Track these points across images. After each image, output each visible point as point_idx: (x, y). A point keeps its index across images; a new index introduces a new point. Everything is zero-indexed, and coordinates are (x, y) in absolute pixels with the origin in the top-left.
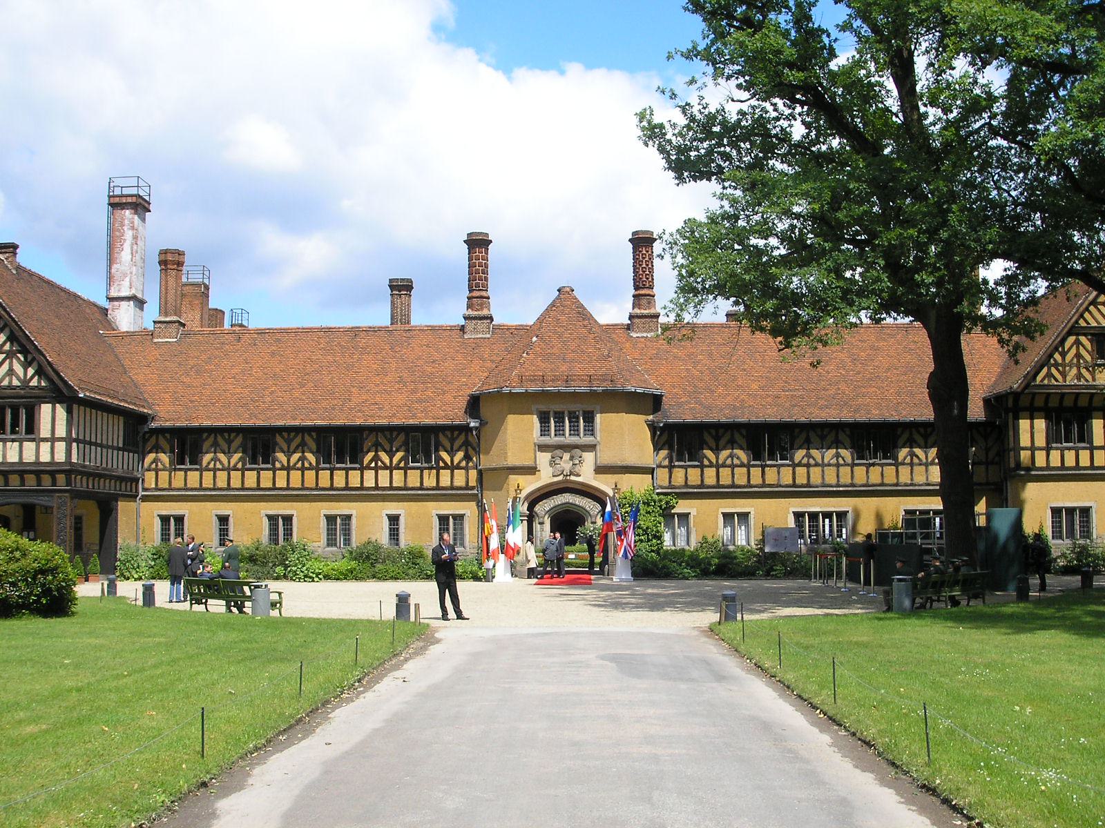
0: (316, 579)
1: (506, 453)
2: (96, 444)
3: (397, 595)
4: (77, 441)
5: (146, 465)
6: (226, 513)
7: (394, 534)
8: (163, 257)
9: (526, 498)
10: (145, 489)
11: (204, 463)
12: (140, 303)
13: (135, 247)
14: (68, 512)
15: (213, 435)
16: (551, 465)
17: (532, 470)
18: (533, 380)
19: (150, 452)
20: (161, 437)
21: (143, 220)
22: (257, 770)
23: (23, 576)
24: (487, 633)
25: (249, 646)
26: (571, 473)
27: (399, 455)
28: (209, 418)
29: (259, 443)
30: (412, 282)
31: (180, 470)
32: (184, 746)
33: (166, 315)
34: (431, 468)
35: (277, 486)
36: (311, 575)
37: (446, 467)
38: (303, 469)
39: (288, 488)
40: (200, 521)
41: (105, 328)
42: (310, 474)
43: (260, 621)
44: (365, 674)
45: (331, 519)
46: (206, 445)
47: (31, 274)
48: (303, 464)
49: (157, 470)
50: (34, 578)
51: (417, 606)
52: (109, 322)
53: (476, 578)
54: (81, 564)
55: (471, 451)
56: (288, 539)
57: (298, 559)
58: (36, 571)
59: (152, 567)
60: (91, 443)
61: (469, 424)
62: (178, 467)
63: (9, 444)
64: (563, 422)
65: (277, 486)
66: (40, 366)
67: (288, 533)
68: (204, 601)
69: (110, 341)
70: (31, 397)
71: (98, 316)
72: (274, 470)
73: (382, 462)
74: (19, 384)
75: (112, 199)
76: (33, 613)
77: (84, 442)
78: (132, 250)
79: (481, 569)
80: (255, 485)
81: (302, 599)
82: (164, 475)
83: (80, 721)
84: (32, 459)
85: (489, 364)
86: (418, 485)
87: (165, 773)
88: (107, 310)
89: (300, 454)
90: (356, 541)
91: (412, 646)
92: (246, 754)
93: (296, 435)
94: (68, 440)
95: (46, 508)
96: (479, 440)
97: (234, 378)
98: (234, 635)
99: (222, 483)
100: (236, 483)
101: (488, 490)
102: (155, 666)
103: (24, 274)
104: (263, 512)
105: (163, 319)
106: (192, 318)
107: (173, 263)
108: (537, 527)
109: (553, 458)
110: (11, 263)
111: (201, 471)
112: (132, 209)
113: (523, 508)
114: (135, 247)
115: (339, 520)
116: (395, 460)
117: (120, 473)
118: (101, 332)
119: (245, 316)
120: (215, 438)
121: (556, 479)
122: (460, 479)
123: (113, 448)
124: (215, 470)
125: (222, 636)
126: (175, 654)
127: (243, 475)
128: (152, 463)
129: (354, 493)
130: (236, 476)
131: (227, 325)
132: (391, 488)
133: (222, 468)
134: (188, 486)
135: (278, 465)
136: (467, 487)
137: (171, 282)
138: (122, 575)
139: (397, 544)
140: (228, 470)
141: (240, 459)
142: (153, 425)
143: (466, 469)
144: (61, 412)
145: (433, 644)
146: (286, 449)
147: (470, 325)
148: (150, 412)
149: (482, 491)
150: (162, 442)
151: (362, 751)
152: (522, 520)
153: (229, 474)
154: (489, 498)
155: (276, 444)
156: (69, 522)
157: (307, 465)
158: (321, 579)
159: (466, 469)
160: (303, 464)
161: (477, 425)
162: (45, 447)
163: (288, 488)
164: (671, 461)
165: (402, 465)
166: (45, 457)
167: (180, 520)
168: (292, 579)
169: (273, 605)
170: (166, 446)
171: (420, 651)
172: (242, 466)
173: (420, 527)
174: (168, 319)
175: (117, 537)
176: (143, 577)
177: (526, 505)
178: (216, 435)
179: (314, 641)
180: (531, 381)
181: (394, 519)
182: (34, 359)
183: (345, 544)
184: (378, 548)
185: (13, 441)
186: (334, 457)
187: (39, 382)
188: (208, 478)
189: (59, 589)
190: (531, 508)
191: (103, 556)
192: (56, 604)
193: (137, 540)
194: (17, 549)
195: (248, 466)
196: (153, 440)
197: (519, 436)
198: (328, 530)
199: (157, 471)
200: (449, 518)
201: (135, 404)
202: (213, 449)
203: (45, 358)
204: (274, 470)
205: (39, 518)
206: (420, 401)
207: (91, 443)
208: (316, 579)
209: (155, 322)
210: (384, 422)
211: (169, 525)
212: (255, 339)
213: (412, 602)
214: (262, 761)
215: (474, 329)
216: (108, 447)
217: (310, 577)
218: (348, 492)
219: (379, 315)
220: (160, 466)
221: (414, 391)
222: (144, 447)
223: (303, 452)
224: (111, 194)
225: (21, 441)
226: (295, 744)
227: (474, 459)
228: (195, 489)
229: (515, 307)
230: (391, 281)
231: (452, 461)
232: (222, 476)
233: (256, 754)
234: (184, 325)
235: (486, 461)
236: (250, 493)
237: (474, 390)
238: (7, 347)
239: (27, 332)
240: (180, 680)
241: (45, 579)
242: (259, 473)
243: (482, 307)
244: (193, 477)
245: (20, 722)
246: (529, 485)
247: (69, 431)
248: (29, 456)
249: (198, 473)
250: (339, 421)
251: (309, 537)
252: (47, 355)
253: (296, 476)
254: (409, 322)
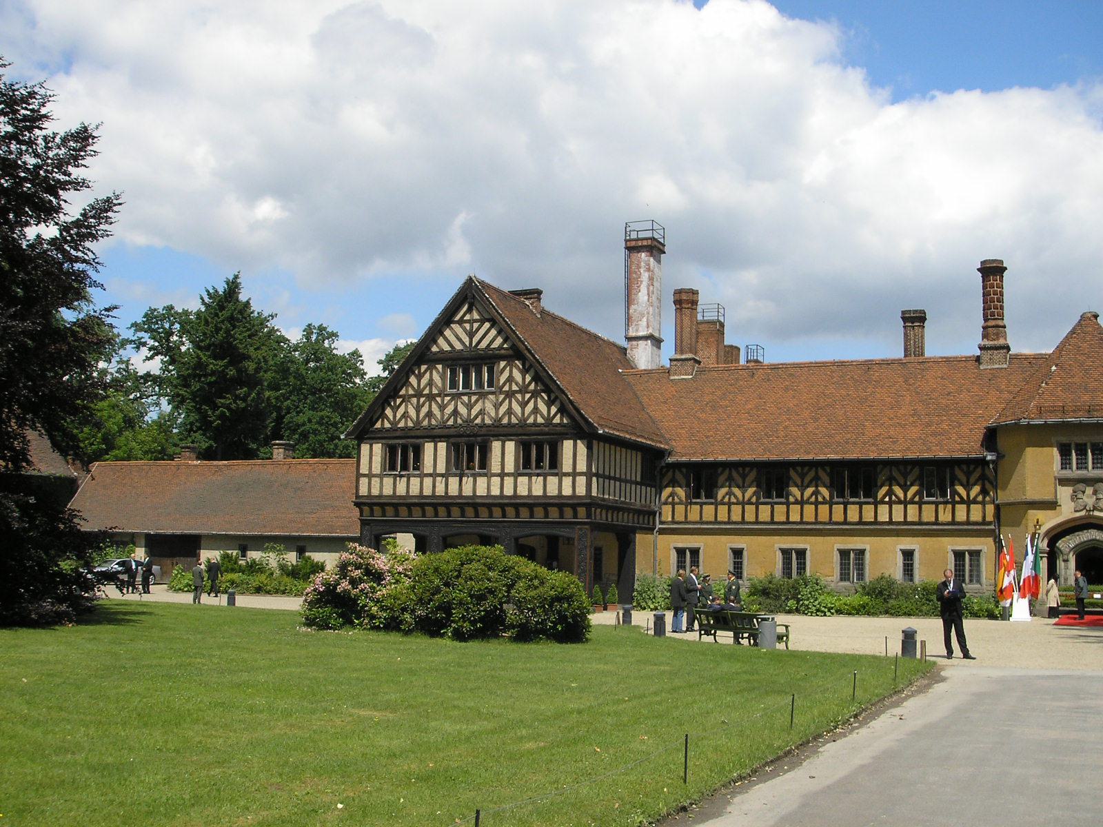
0: (828, 614)
1: (1025, 487)
2: (615, 479)
3: (903, 632)
4: (597, 475)
5: (663, 499)
6: (740, 546)
7: (908, 570)
8: (677, 297)
9: (1046, 534)
10: (661, 523)
11: (719, 497)
12: (657, 342)
13: (651, 288)
14: (589, 544)
15: (728, 470)
16: (1072, 500)
17: (1052, 505)
18: (1052, 411)
19: (667, 486)
20: (677, 472)
21: (659, 262)
22: (738, 799)
23: (540, 603)
24: (996, 674)
25: (751, 678)
26: (1095, 508)
27: (914, 489)
28: (723, 453)
29: (773, 478)
30: (925, 313)
31: (696, 503)
32: (669, 771)
33: (682, 353)
34: (946, 503)
35: (791, 520)
36: (823, 609)
37: (962, 501)
38: (816, 503)
39: (802, 522)
40: (715, 554)
41: (624, 367)
42: (824, 509)
43: (765, 654)
44: (862, 711)
45: (844, 554)
46: (721, 479)
47: (554, 317)
48: (817, 498)
49: (673, 504)
50: (551, 605)
51: (923, 643)
52: (628, 361)
53: (992, 616)
54: (600, 593)
55: (988, 486)
56: (800, 574)
57: (810, 593)
58: (552, 599)
59: (668, 598)
60: (610, 478)
61: (985, 457)
62: (694, 501)
63: (534, 478)
64: (1086, 454)
65: (791, 520)
66: (562, 404)
67: (802, 567)
68: (713, 632)
69: (630, 379)
70: (553, 434)
71: (618, 355)
72: (788, 504)
73: (896, 496)
74: (543, 421)
75: (628, 243)
76: (550, 639)
77: (604, 477)
78: (648, 291)
79: (997, 607)
80: (769, 519)
81: (808, 633)
82: (680, 509)
83: (575, 742)
84: (555, 493)
85: (1006, 395)
86: (933, 519)
87: (646, 795)
88: (626, 349)
89: (814, 489)
90: (869, 575)
91: (916, 684)
92: (730, 783)
93: (810, 470)
94: (589, 475)
95: (568, 539)
96: (996, 472)
97: (748, 413)
98: (737, 667)
99: (736, 517)
100: (750, 517)
101: (1004, 526)
102: (655, 693)
103: (548, 318)
104: (777, 546)
105: (678, 357)
106: (708, 356)
107: (688, 302)
108: (1060, 564)
109: (1074, 492)
110: (536, 308)
111: (716, 504)
112: (648, 251)
113: (1044, 545)
114: (651, 288)
115: (852, 555)
116: (910, 494)
117: (638, 506)
118: (620, 371)
119: (761, 351)
120: (730, 473)
121: (1078, 514)
122: (976, 515)
123: (631, 482)
124: (729, 504)
125: (725, 667)
126: (677, 682)
127: (757, 509)
128: (669, 497)
129: (867, 527)
130: (750, 509)
131: (742, 361)
132: (905, 523)
133: (736, 502)
135: (791, 499)
136: (984, 522)
137: (686, 321)
138: (639, 604)
139: (912, 580)
140: (743, 504)
141: (755, 493)
142: (670, 460)
143: (983, 503)
144: (582, 448)
145: (937, 682)
146: (799, 484)
147: (986, 356)
148: (667, 447)
149: (999, 526)
150: (679, 476)
151: (844, 786)
152: (1042, 557)
153: (743, 508)
154: (1006, 535)
155: (789, 478)
156: (589, 553)
157: (820, 499)
158: (833, 614)
159: (983, 503)
160: (817, 498)
161: (994, 458)
162: (567, 482)
163: (802, 522)
165: (917, 499)
166: (567, 491)
167: (695, 552)
168: (804, 613)
169: (780, 638)
170: (683, 481)
171: (922, 690)
172: (757, 500)
173: (934, 561)
174: (683, 357)
175: (634, 569)
176: (659, 608)
177: (1046, 541)
178: (730, 469)
179: (815, 675)
180: (1051, 412)
181: (908, 555)
182: (556, 398)
183: (858, 579)
184: (891, 583)
185: (538, 475)
186: (847, 492)
187: (561, 419)
188: (723, 512)
189: (574, 616)
190: (1052, 542)
191: (618, 584)
192: (572, 630)
193: (654, 572)
194: (536, 577)
195: (762, 500)
196: (670, 474)
197: (1039, 469)
198: (841, 564)
199: (673, 504)
200: (965, 553)
201: (653, 440)
202: (727, 484)
203: (567, 396)
204: (788, 504)
205: (562, 548)
206: (934, 434)
207: (610, 478)
208: (828, 614)
209: (671, 360)
210: (898, 456)
211: (685, 558)
212: (768, 375)
213: (919, 638)
214: (744, 790)
215: (990, 359)
216: (626, 481)
217: (822, 612)
218: (862, 527)
219: (889, 346)
220: (676, 500)
221: (929, 425)
222: (661, 482)
223: (817, 486)
224: (628, 238)
225: (545, 476)
226: (779, 776)
227: (991, 493)
228: (710, 523)
229: (1031, 338)
230: (903, 312)
231: (968, 495)
232: (737, 510)
233: (739, 783)
234: (699, 362)
235: (1003, 497)
236: (764, 527)
237: (991, 422)
238: (532, 387)
239: (550, 373)
240: (677, 707)
241: (561, 606)
242: (772, 507)
243: (998, 336)
244: (709, 511)
245: (522, 738)
246: (1049, 520)
247: (589, 466)
248: (552, 490)
249: (713, 507)
250: (853, 456)
251: (822, 572)
252: (568, 394)
253: (809, 510)
254: (923, 354)
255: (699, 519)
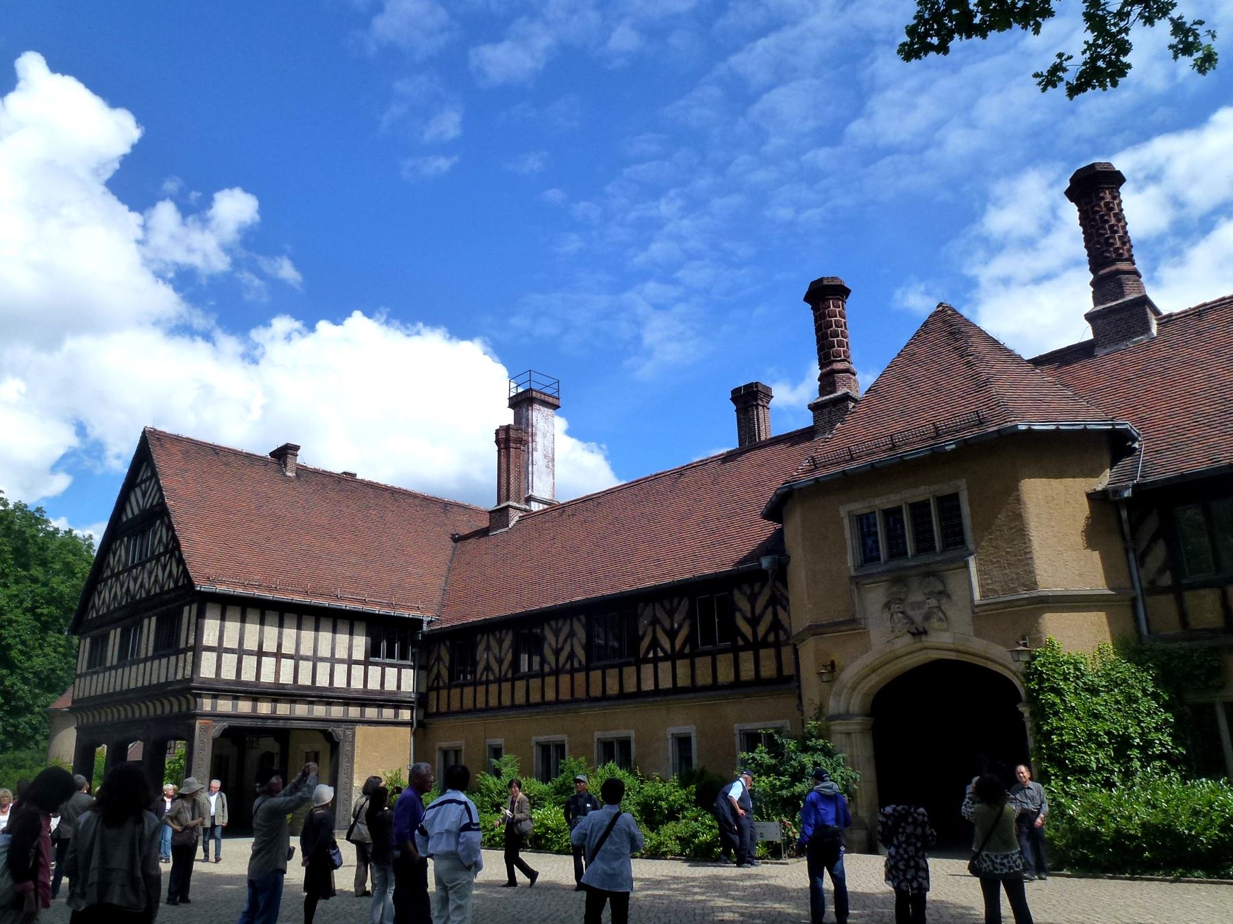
73: (663, 650)
164: (1176, 577)
165: (687, 650)
231: (755, 633)
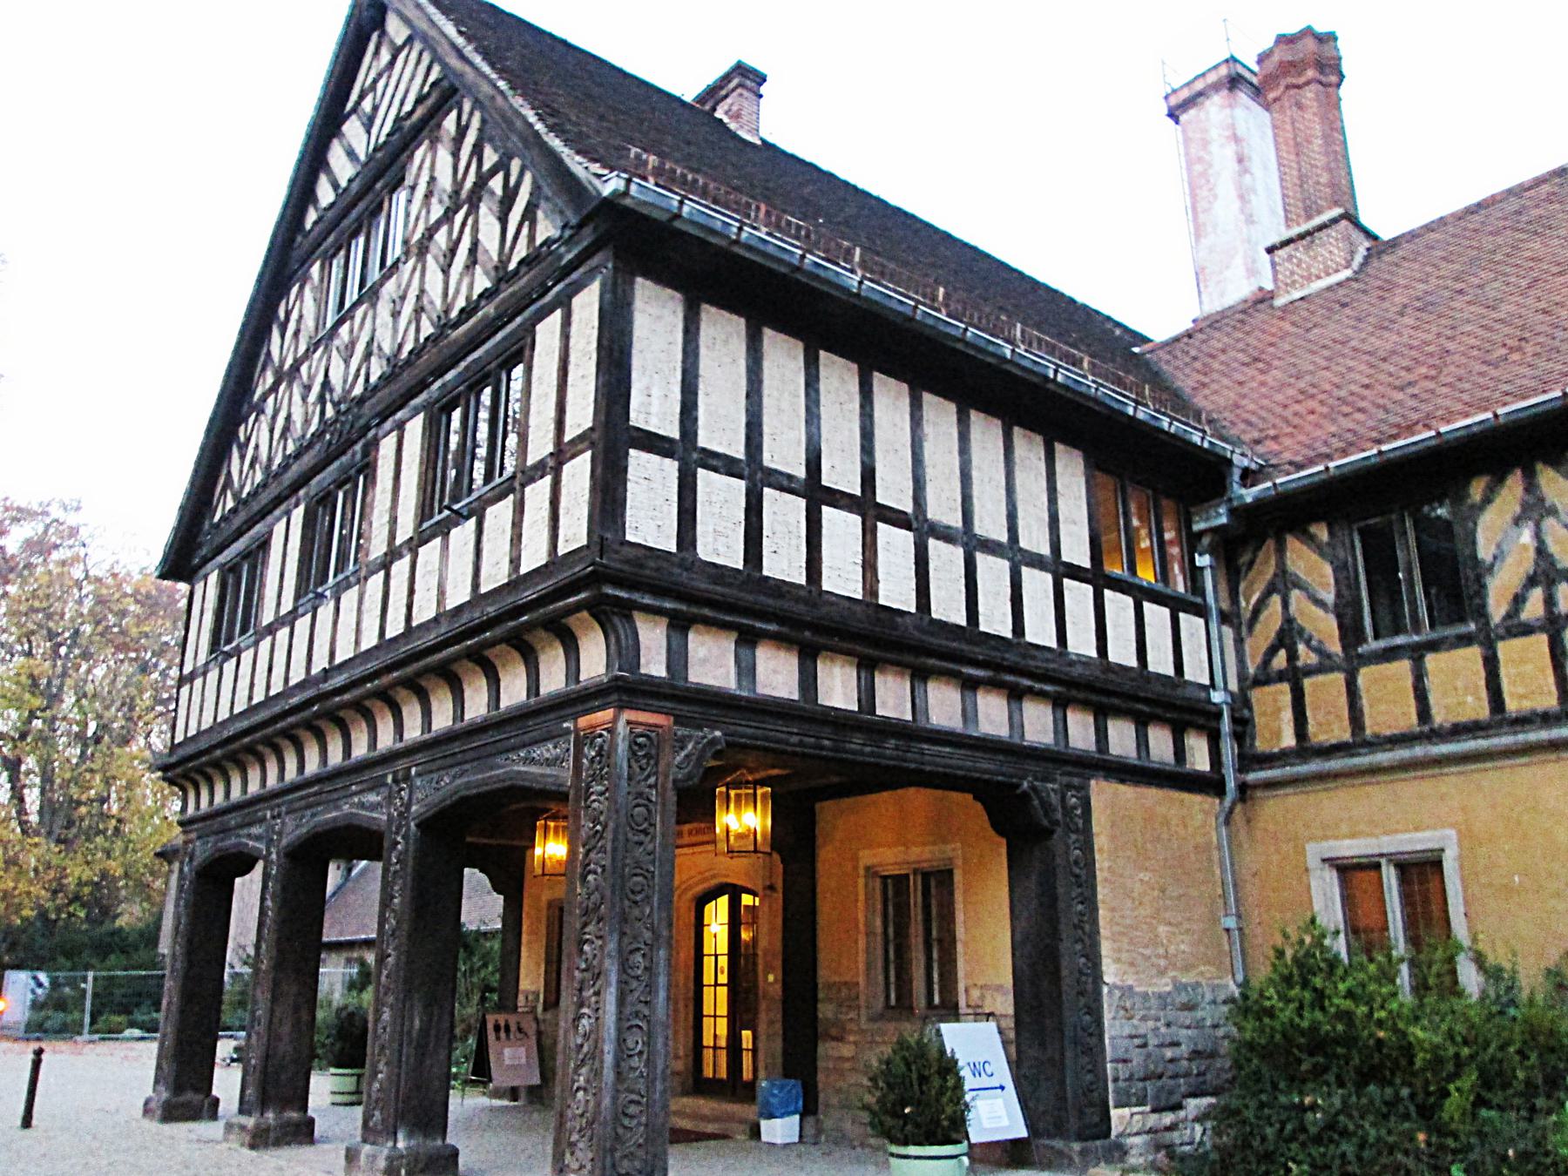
11: (1497, 610)
128: (1272, 651)
134: (1439, 717)
199: (1294, 676)
220: (1306, 657)
249: (1474, 653)
255: (1414, 719)
